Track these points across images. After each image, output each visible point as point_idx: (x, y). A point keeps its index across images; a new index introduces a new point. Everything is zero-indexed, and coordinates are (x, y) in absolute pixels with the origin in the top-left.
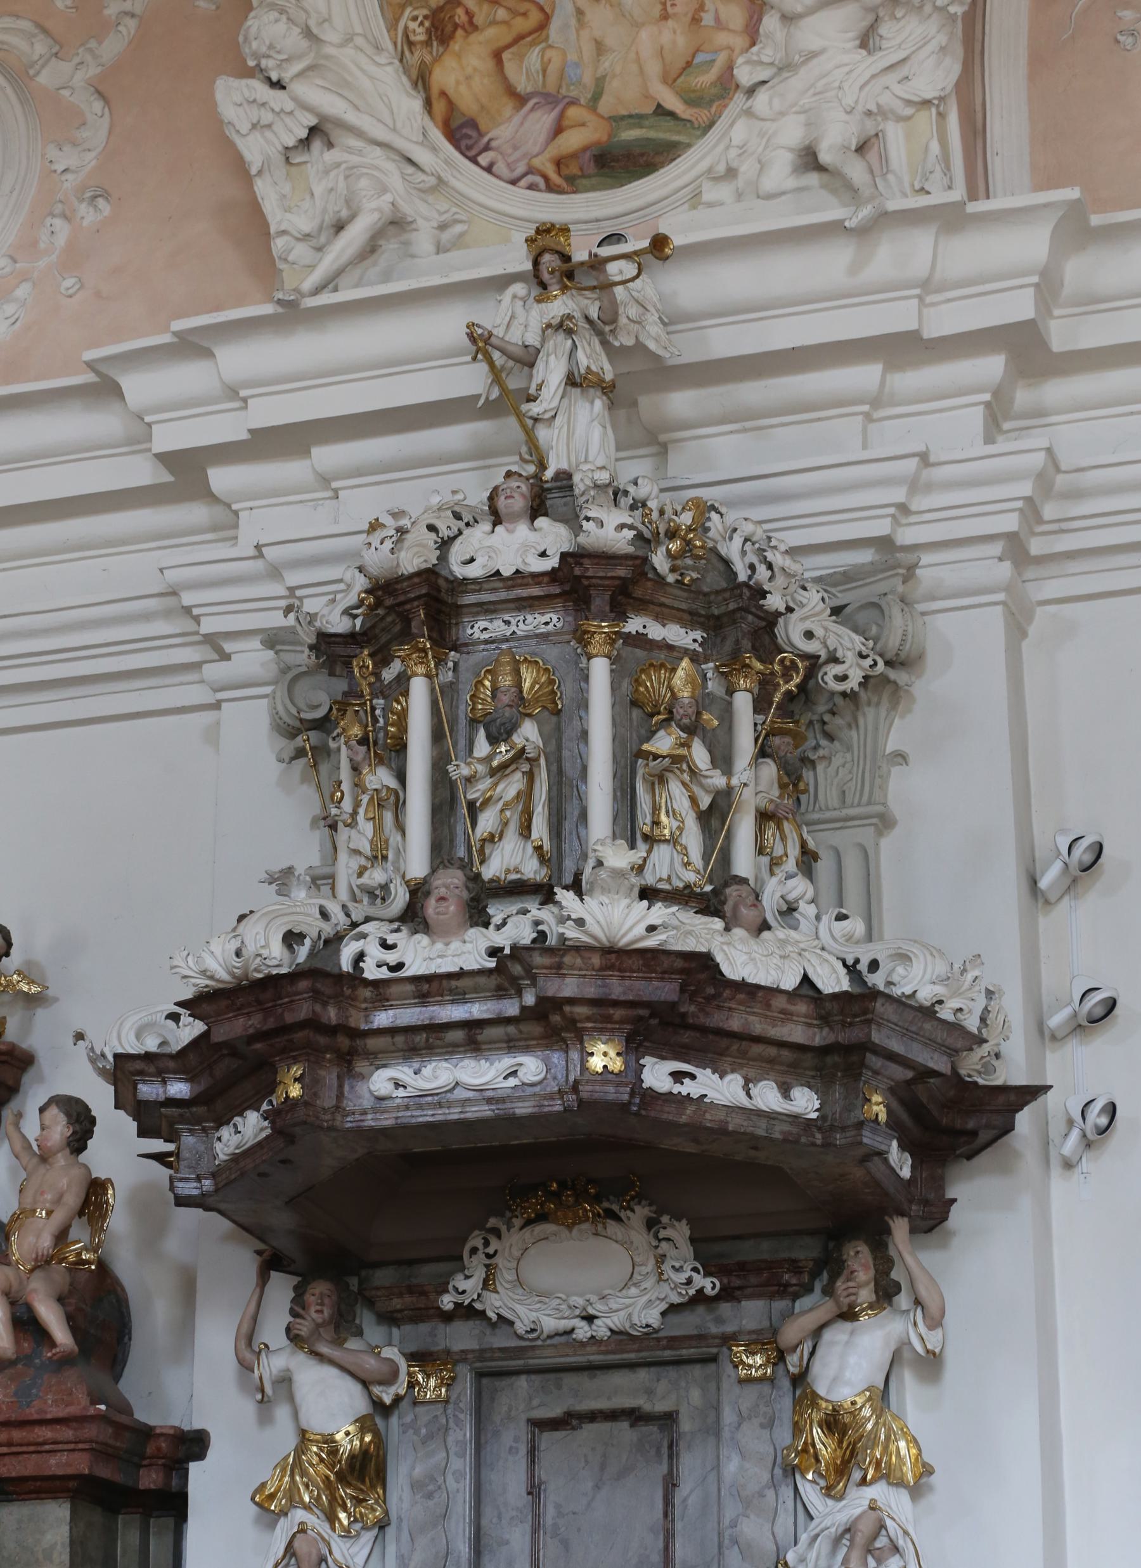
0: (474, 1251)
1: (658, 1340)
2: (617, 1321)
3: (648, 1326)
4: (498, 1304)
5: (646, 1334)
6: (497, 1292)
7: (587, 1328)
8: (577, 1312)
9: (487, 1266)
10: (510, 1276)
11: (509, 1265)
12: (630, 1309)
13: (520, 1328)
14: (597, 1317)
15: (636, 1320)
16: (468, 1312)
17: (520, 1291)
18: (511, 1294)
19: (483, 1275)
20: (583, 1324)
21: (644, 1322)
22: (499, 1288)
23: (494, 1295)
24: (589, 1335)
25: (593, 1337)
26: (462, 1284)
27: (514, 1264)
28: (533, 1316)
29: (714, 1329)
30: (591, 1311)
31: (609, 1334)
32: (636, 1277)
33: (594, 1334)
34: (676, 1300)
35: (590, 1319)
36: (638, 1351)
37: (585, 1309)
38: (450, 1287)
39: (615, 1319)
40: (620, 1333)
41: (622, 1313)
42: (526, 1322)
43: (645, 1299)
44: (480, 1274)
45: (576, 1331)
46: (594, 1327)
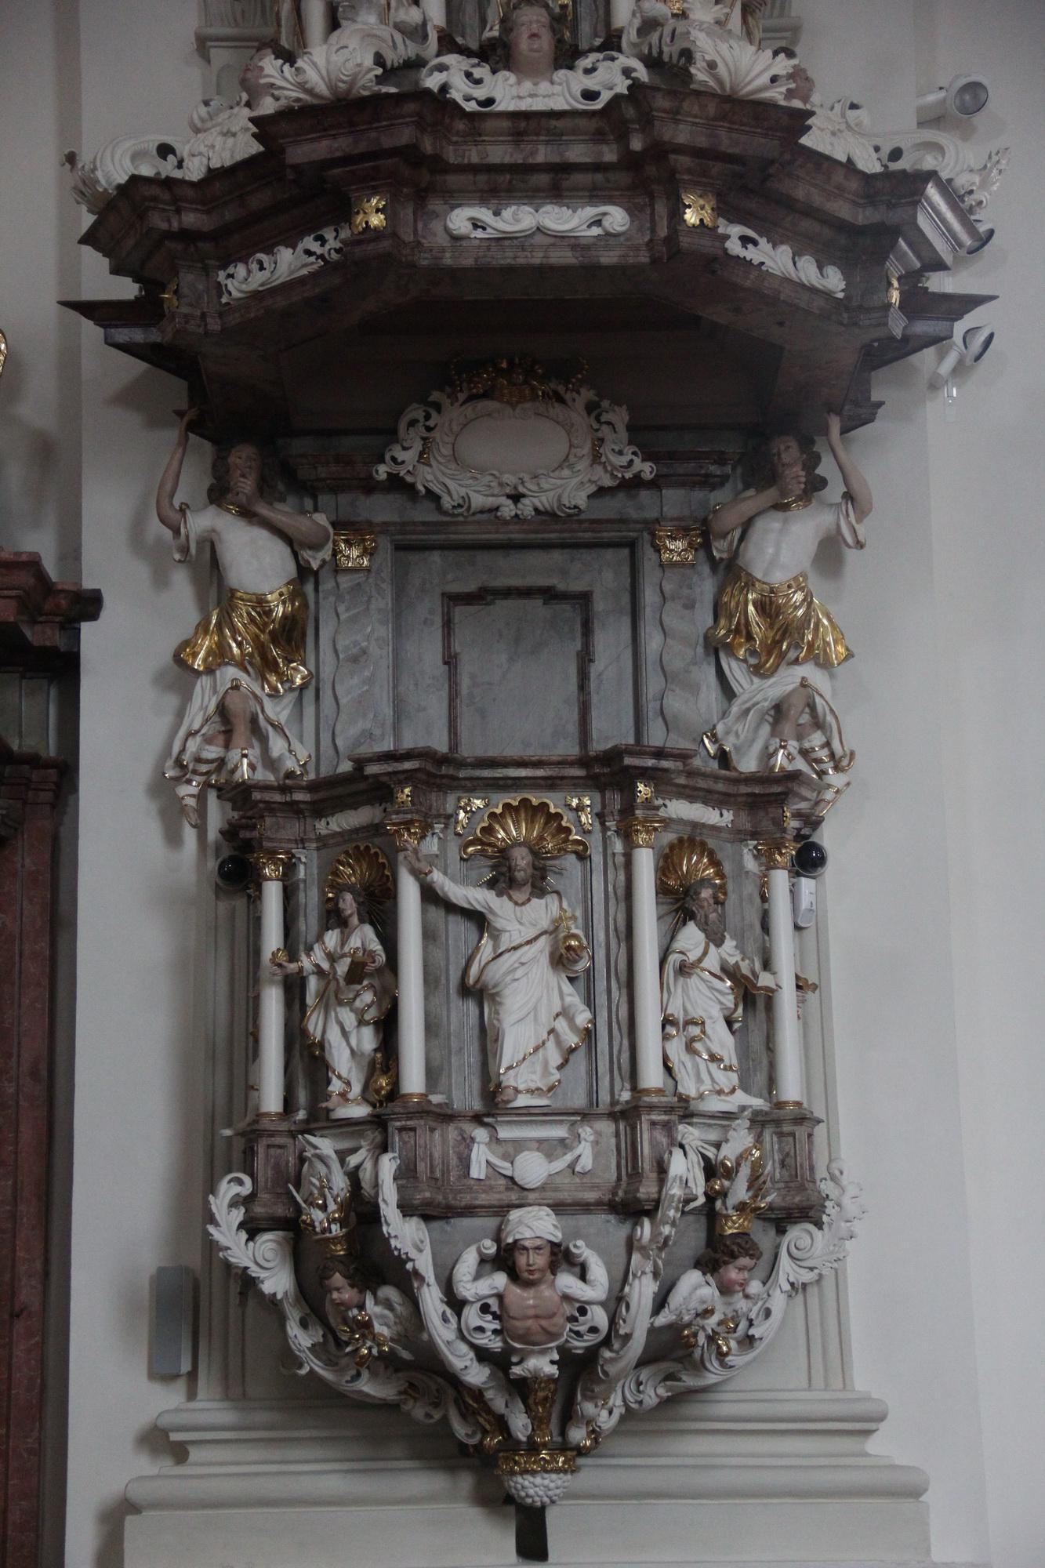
0: (412, 423)
1: (581, 522)
2: (544, 501)
3: (575, 507)
4: (429, 477)
5: (569, 515)
6: (430, 466)
7: (512, 506)
8: (508, 490)
9: (424, 439)
10: (446, 451)
11: (446, 439)
12: (560, 491)
13: (447, 502)
14: (524, 496)
15: (566, 502)
16: (396, 484)
17: (453, 466)
18: (443, 468)
19: (421, 448)
20: (509, 502)
21: (573, 503)
22: (433, 462)
23: (427, 469)
24: (513, 513)
25: (517, 515)
26: (401, 455)
27: (450, 439)
28: (463, 491)
29: (634, 514)
30: (521, 489)
31: (533, 513)
32: (572, 459)
33: (519, 512)
34: (607, 482)
35: (516, 498)
36: (561, 531)
37: (515, 488)
38: (387, 457)
39: (544, 499)
40: (546, 513)
41: (551, 494)
42: (455, 497)
43: (575, 481)
44: (418, 446)
45: (502, 509)
46: (520, 505)
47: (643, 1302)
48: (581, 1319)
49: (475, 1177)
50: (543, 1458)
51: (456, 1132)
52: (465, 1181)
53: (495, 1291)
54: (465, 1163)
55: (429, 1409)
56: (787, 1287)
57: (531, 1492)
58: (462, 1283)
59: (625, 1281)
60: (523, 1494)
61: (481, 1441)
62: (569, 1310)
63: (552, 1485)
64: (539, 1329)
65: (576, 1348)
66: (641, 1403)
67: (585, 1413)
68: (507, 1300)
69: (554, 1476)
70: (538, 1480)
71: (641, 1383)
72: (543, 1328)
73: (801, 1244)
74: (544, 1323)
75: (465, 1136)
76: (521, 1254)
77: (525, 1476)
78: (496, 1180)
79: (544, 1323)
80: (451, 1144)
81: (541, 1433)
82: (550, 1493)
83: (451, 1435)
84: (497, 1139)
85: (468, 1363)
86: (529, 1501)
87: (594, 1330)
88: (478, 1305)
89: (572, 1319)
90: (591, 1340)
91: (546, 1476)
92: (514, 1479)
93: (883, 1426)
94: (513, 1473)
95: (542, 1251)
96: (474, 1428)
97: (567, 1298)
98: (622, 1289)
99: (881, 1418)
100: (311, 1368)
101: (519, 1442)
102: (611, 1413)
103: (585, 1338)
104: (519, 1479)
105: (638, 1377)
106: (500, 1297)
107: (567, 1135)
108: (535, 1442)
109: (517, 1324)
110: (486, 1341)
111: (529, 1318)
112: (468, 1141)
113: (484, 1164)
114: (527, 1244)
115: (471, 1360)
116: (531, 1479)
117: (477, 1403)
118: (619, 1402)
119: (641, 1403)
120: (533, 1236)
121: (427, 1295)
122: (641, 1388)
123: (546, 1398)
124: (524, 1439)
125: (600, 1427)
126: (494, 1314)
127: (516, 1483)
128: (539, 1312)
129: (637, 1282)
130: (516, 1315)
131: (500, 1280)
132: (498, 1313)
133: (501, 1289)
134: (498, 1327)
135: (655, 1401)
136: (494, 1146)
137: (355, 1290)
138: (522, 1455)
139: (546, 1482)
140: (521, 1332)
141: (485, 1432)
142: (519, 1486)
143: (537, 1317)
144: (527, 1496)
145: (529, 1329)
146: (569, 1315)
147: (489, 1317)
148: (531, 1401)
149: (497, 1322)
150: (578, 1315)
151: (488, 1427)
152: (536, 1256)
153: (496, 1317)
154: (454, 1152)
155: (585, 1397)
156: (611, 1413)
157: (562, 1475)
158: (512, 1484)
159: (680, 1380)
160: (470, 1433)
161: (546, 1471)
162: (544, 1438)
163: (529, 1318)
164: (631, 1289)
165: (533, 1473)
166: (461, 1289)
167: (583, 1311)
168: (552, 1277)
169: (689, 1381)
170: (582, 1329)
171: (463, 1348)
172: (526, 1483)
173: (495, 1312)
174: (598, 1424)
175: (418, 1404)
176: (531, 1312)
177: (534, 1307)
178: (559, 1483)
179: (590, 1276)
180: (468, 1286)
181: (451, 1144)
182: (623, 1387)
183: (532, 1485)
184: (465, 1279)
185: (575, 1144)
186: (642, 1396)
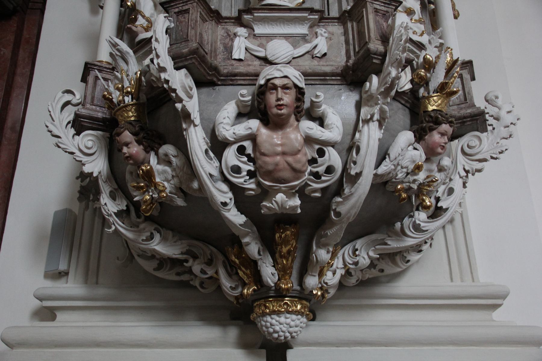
47: (371, 142)
48: (320, 160)
49: (237, 58)
50: (286, 303)
51: (223, 31)
52: (228, 61)
53: (249, 132)
54: (229, 50)
55: (203, 266)
56: (463, 174)
57: (277, 328)
58: (222, 125)
59: (356, 128)
60: (271, 330)
61: (242, 292)
62: (310, 153)
63: (292, 323)
64: (286, 165)
65: (315, 191)
66: (356, 264)
67: (319, 259)
68: (259, 139)
69: (294, 317)
70: (282, 319)
71: (357, 250)
72: (289, 164)
73: (472, 144)
74: (290, 159)
75: (230, 33)
76: (271, 93)
77: (273, 316)
78: (253, 61)
79: (290, 159)
80: (219, 37)
81: (285, 282)
82: (291, 329)
83: (219, 288)
84: (255, 35)
85: (228, 201)
86: (276, 335)
87: (330, 170)
88: (235, 147)
89: (313, 161)
90: (328, 180)
91: (288, 315)
92: (265, 319)
93: (506, 302)
94: (264, 314)
95: (288, 91)
96: (237, 283)
97: (309, 140)
98: (354, 135)
99: (504, 297)
100: (116, 228)
101: (269, 288)
102: (334, 273)
103: (323, 178)
104: (269, 319)
105: (355, 246)
106: (253, 138)
107: (307, 33)
108: (281, 287)
109: (267, 159)
110: (242, 180)
111: (277, 154)
112: (232, 37)
113: (243, 50)
114: (277, 82)
115: (231, 199)
116: (278, 319)
117: (238, 259)
118: (341, 265)
119: (356, 264)
120: (282, 75)
121: (194, 134)
122: (357, 253)
123: (289, 252)
124: (273, 285)
125: (326, 283)
126: (248, 156)
127: (267, 322)
128: (286, 149)
129: (366, 127)
130: (266, 152)
131: (254, 124)
132: (252, 155)
133: (255, 130)
134: (252, 169)
135: (367, 262)
136: (251, 39)
137: (142, 147)
138: (271, 301)
139: (288, 321)
140: (270, 168)
141: (244, 285)
142: (268, 324)
143: (284, 154)
144: (275, 332)
145: (277, 165)
146: (310, 158)
147: (245, 159)
148: (277, 255)
149: (252, 164)
150: (317, 156)
151: (245, 278)
152: (283, 94)
153: (251, 159)
154: (221, 43)
155: (319, 246)
156: (334, 273)
157: (299, 317)
158: (263, 323)
159: (386, 244)
160: (233, 286)
161: (289, 312)
162: (287, 284)
163: (277, 154)
164: (360, 135)
165: (278, 313)
166: (221, 130)
167: (321, 153)
168: (296, 123)
169: (393, 244)
170: (321, 169)
171: (224, 187)
172: (274, 322)
173: (249, 155)
174: (326, 281)
175: (196, 262)
176: (279, 149)
177: (281, 145)
178: (298, 322)
179: (327, 122)
180: (228, 127)
181: (219, 37)
182: (344, 254)
183: (277, 323)
184: (225, 121)
185: (313, 39)
186: (358, 258)
